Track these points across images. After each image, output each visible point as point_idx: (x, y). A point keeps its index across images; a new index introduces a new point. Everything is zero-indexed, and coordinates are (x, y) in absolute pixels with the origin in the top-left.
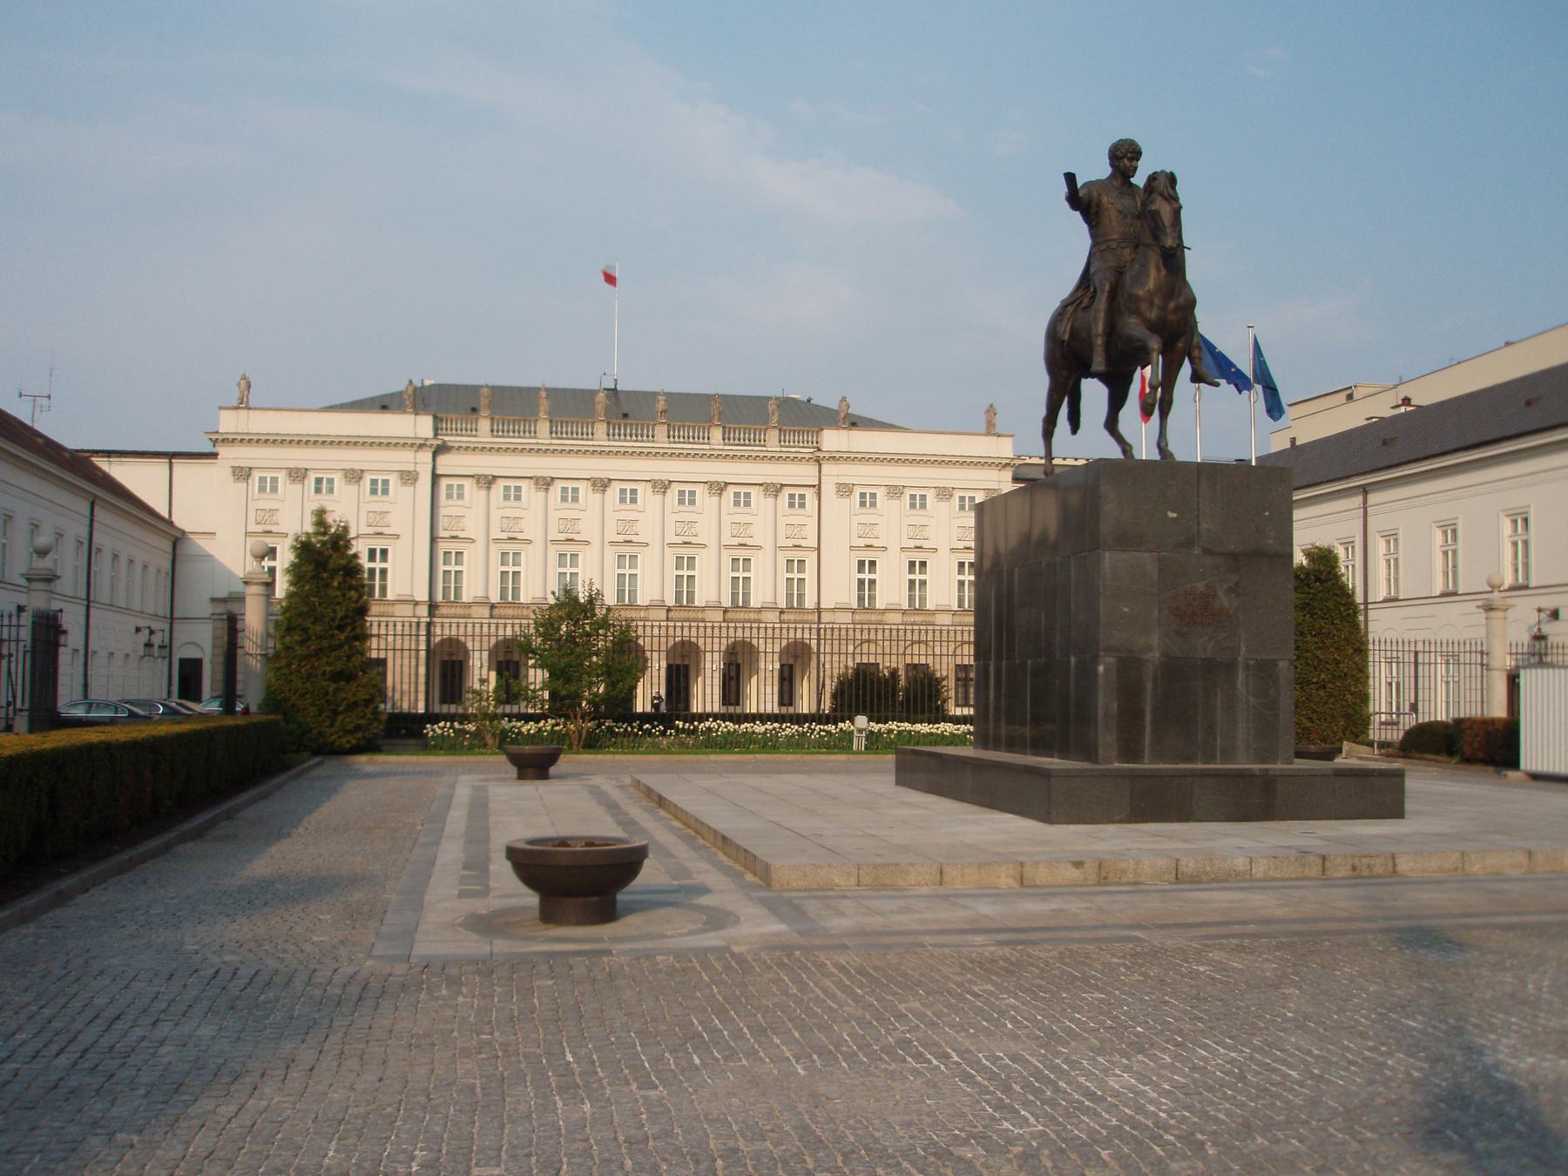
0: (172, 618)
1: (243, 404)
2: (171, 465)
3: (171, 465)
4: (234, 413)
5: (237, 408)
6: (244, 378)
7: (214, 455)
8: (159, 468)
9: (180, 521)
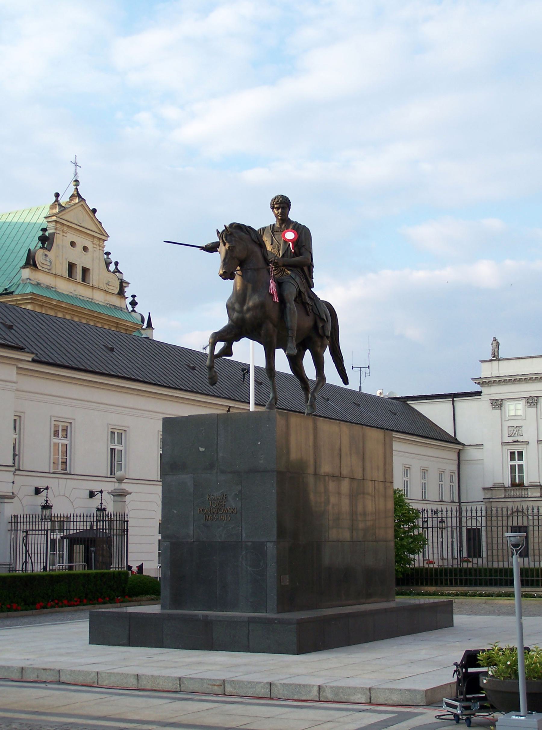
0: (459, 502)
1: (496, 358)
2: (453, 401)
3: (453, 401)
4: (489, 364)
5: (491, 360)
6: (495, 340)
7: (479, 393)
8: (446, 406)
9: (460, 438)
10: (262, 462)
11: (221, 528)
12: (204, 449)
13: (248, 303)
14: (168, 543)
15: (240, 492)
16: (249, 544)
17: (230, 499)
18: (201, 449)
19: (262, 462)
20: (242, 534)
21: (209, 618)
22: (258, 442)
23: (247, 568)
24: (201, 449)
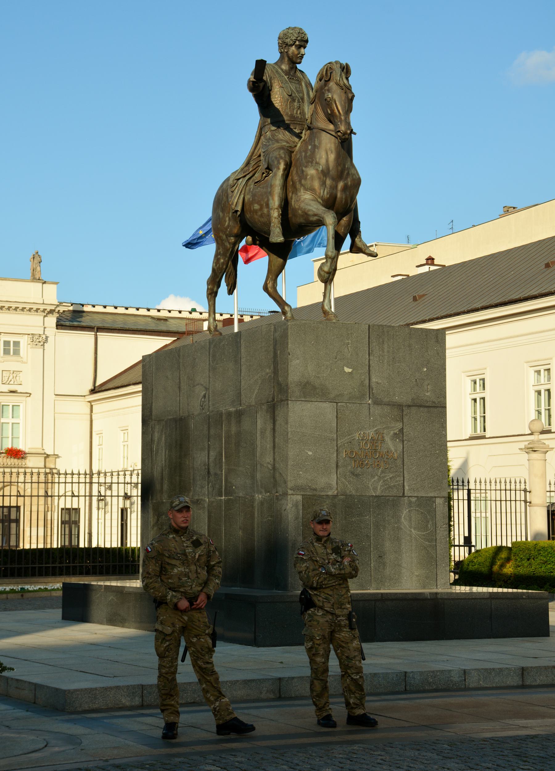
10: (428, 394)
11: (376, 478)
12: (350, 370)
13: (346, 178)
14: (299, 498)
15: (401, 430)
16: (414, 500)
17: (387, 439)
18: (347, 370)
19: (428, 394)
20: (404, 486)
21: (439, 596)
22: (423, 368)
23: (411, 531)
24: (347, 370)
